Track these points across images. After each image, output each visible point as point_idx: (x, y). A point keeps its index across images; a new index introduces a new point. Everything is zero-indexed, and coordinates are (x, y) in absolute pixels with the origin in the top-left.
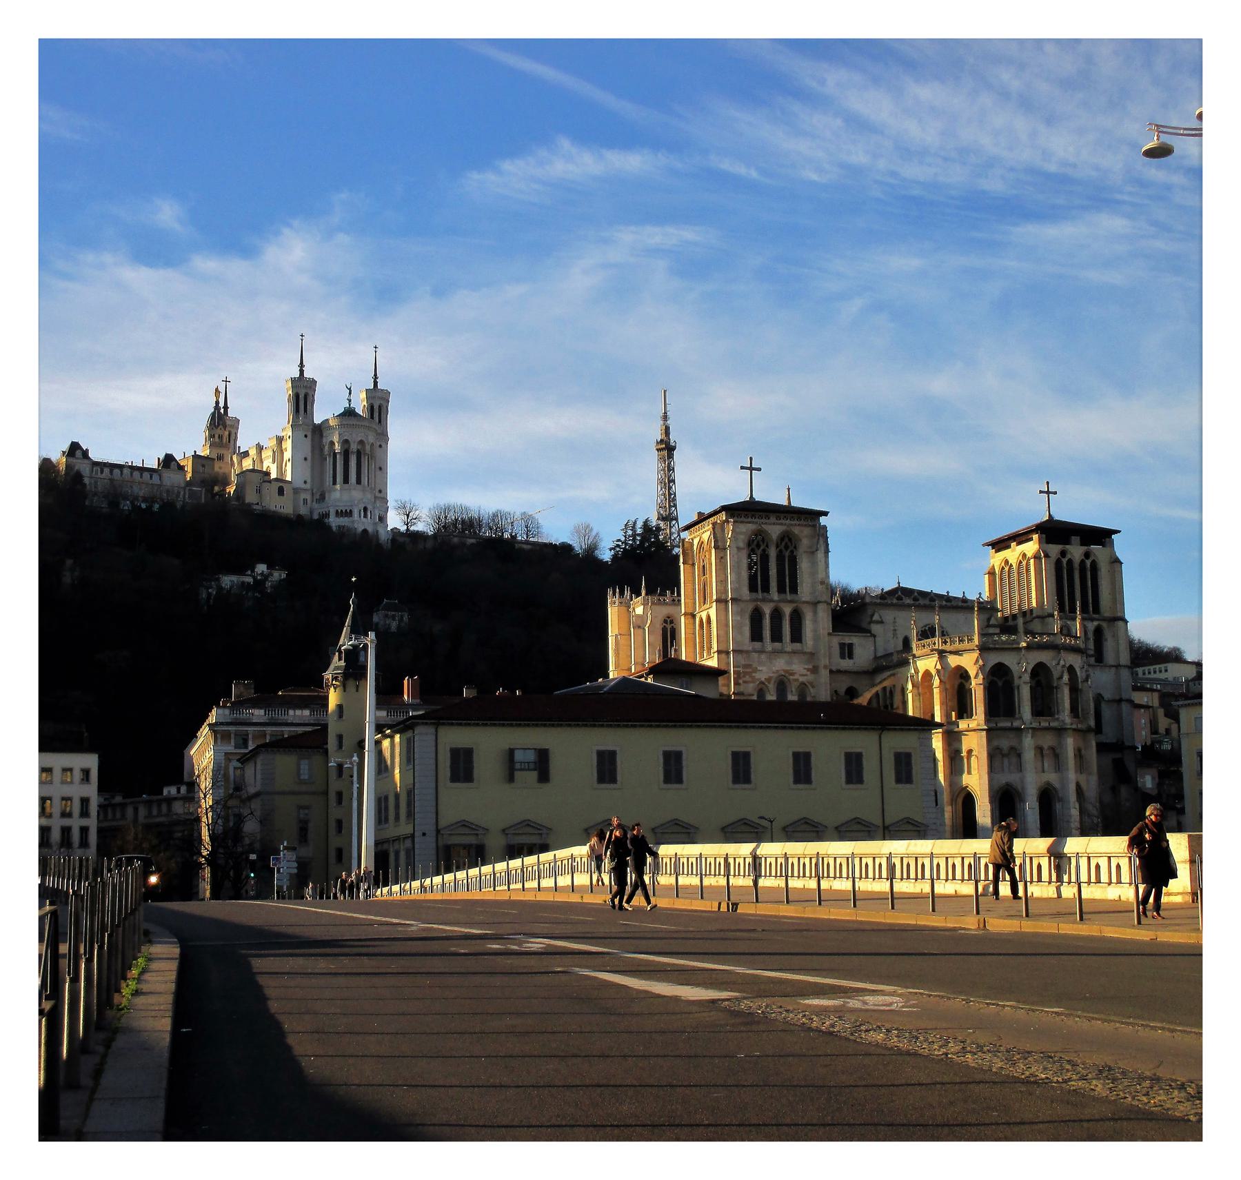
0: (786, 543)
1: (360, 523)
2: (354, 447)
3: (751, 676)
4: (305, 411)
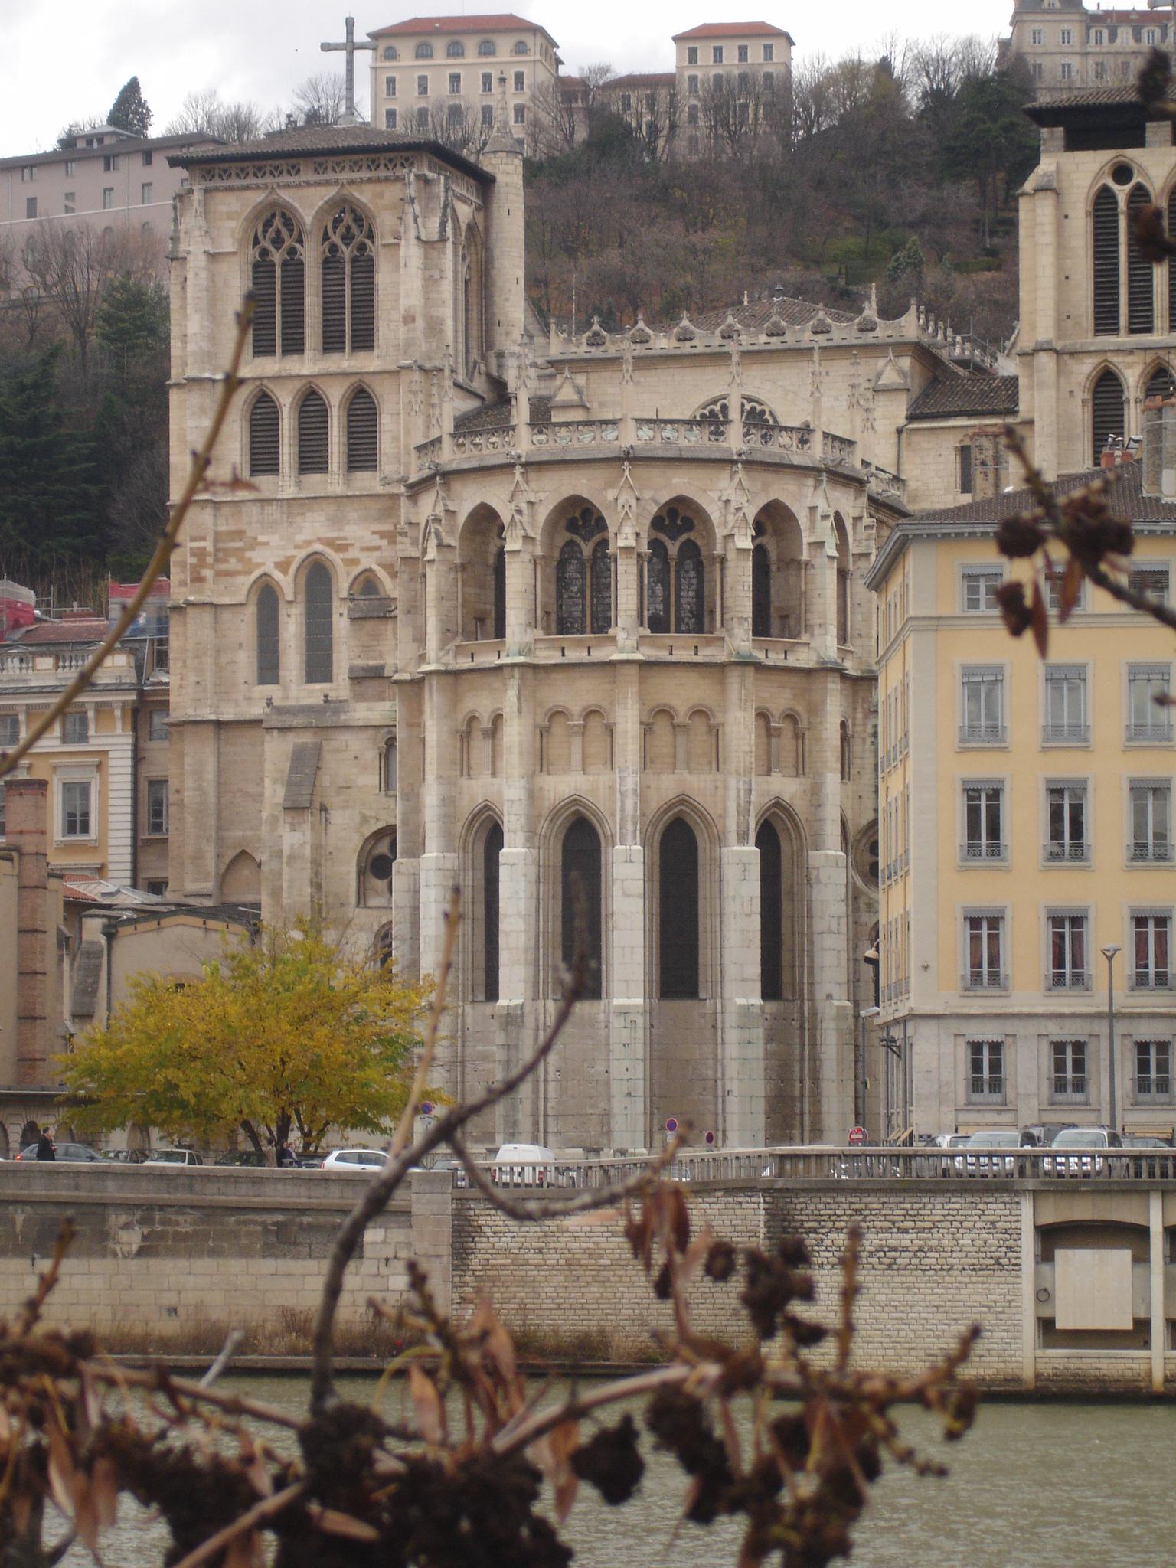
0: (348, 228)
3: (241, 560)
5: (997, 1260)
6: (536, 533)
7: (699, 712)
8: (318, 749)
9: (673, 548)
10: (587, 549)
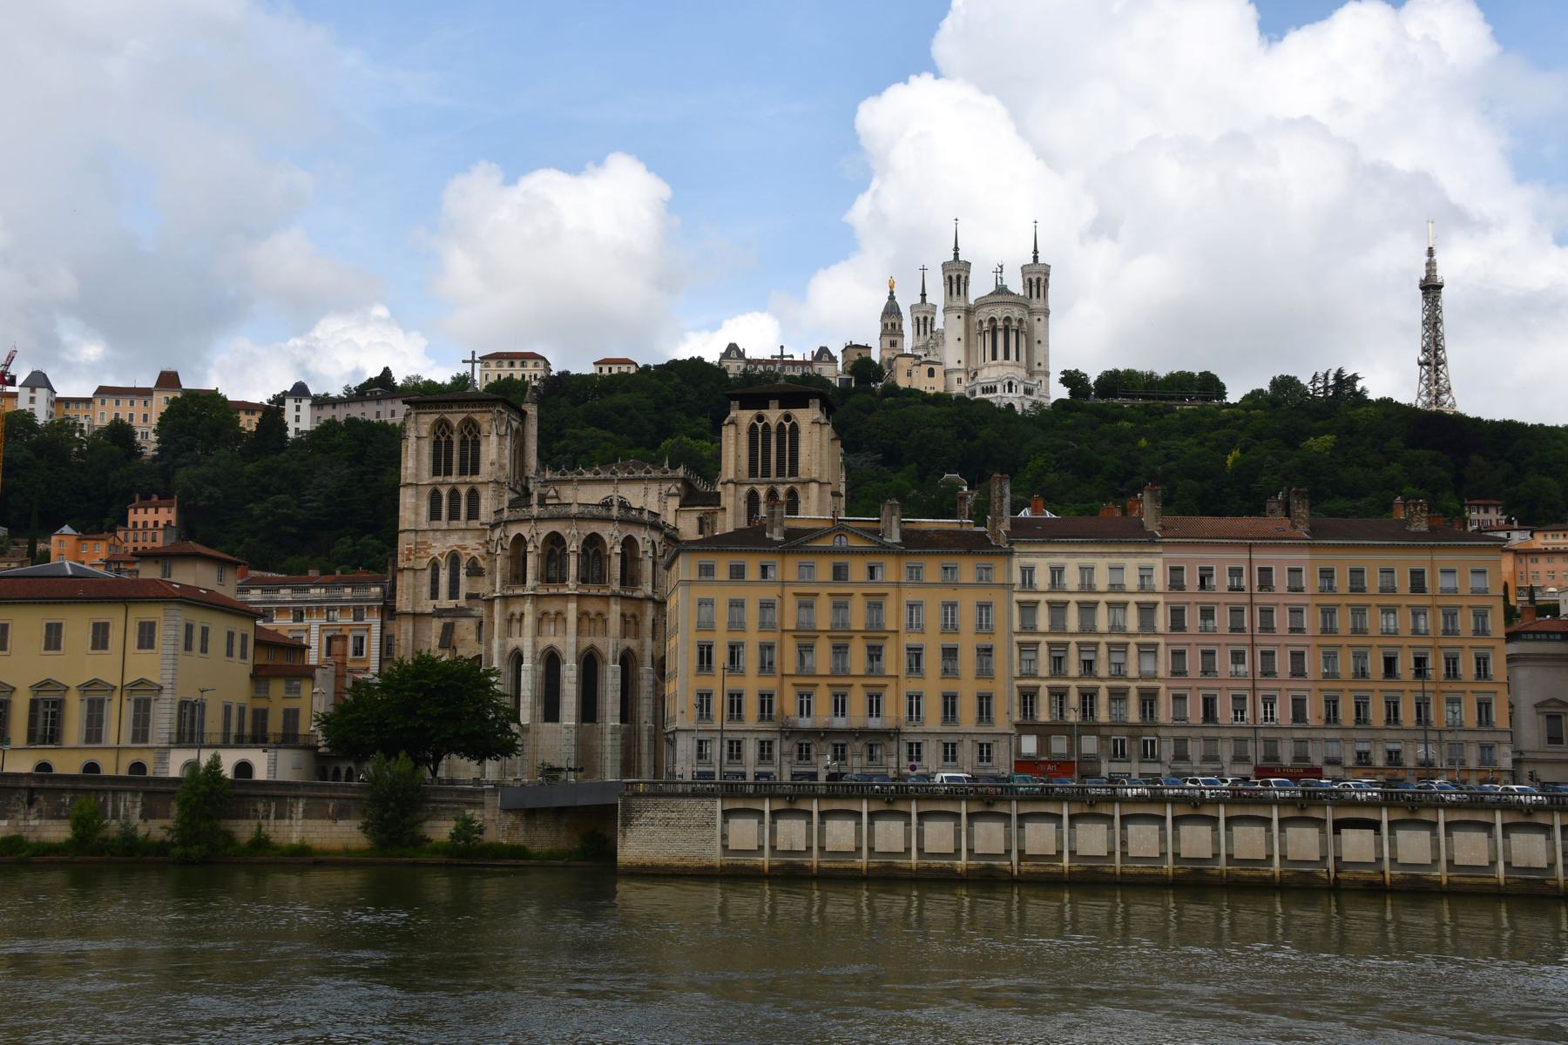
1: (1000, 398)
2: (1000, 324)
4: (959, 293)
5: (708, 823)
6: (539, 545)
7: (599, 614)
8: (453, 625)
9: (591, 552)
10: (558, 552)
